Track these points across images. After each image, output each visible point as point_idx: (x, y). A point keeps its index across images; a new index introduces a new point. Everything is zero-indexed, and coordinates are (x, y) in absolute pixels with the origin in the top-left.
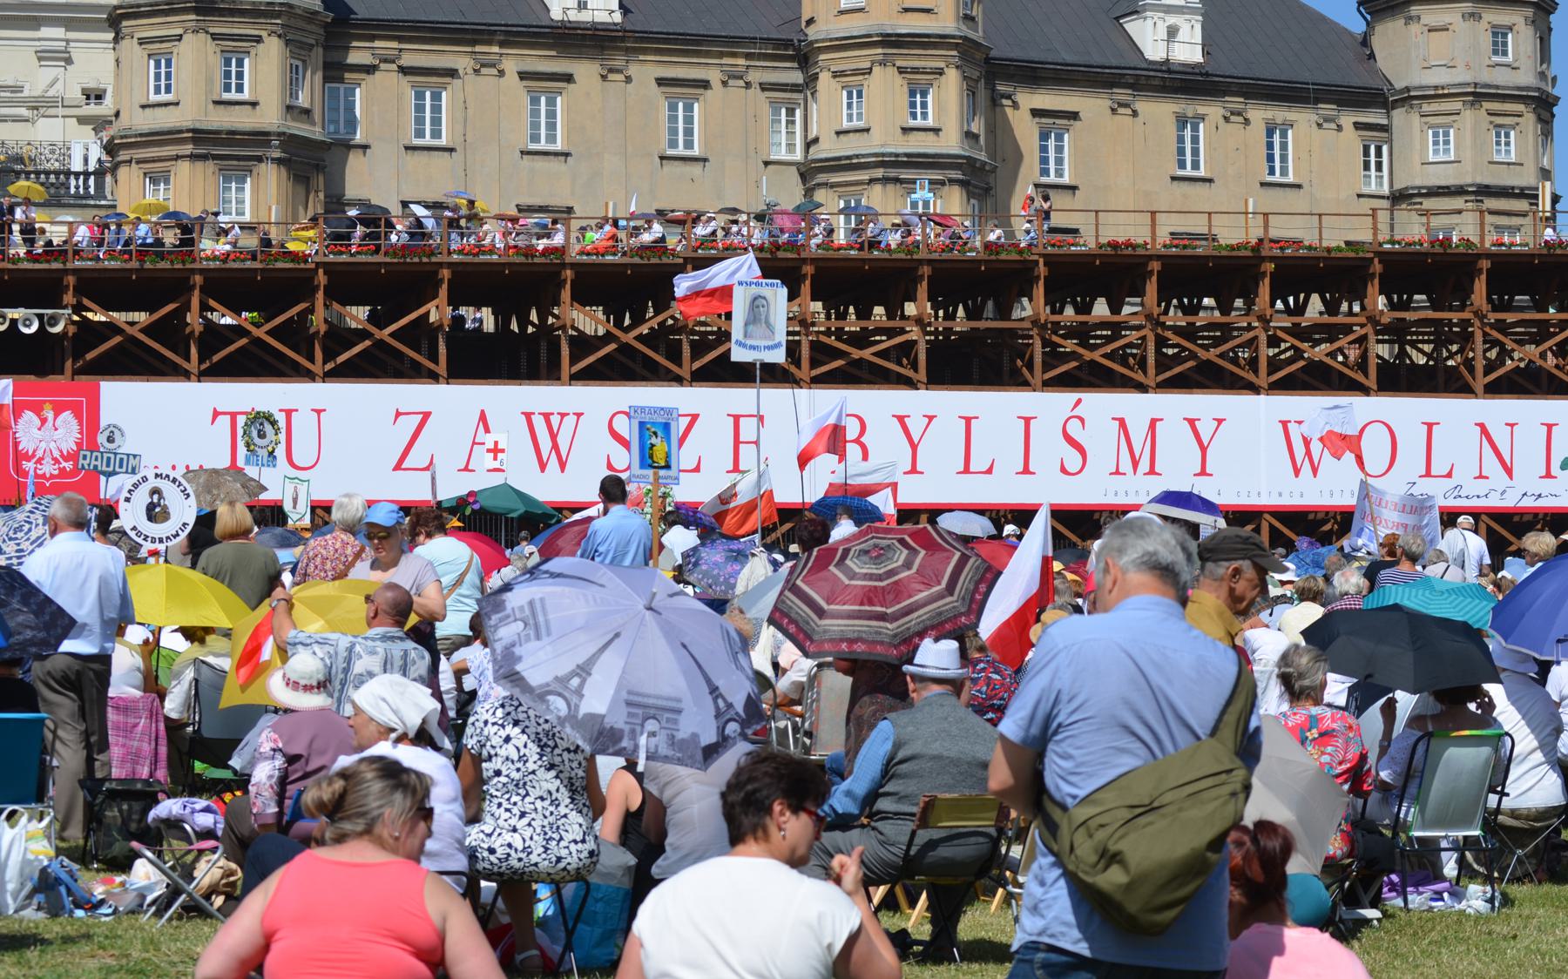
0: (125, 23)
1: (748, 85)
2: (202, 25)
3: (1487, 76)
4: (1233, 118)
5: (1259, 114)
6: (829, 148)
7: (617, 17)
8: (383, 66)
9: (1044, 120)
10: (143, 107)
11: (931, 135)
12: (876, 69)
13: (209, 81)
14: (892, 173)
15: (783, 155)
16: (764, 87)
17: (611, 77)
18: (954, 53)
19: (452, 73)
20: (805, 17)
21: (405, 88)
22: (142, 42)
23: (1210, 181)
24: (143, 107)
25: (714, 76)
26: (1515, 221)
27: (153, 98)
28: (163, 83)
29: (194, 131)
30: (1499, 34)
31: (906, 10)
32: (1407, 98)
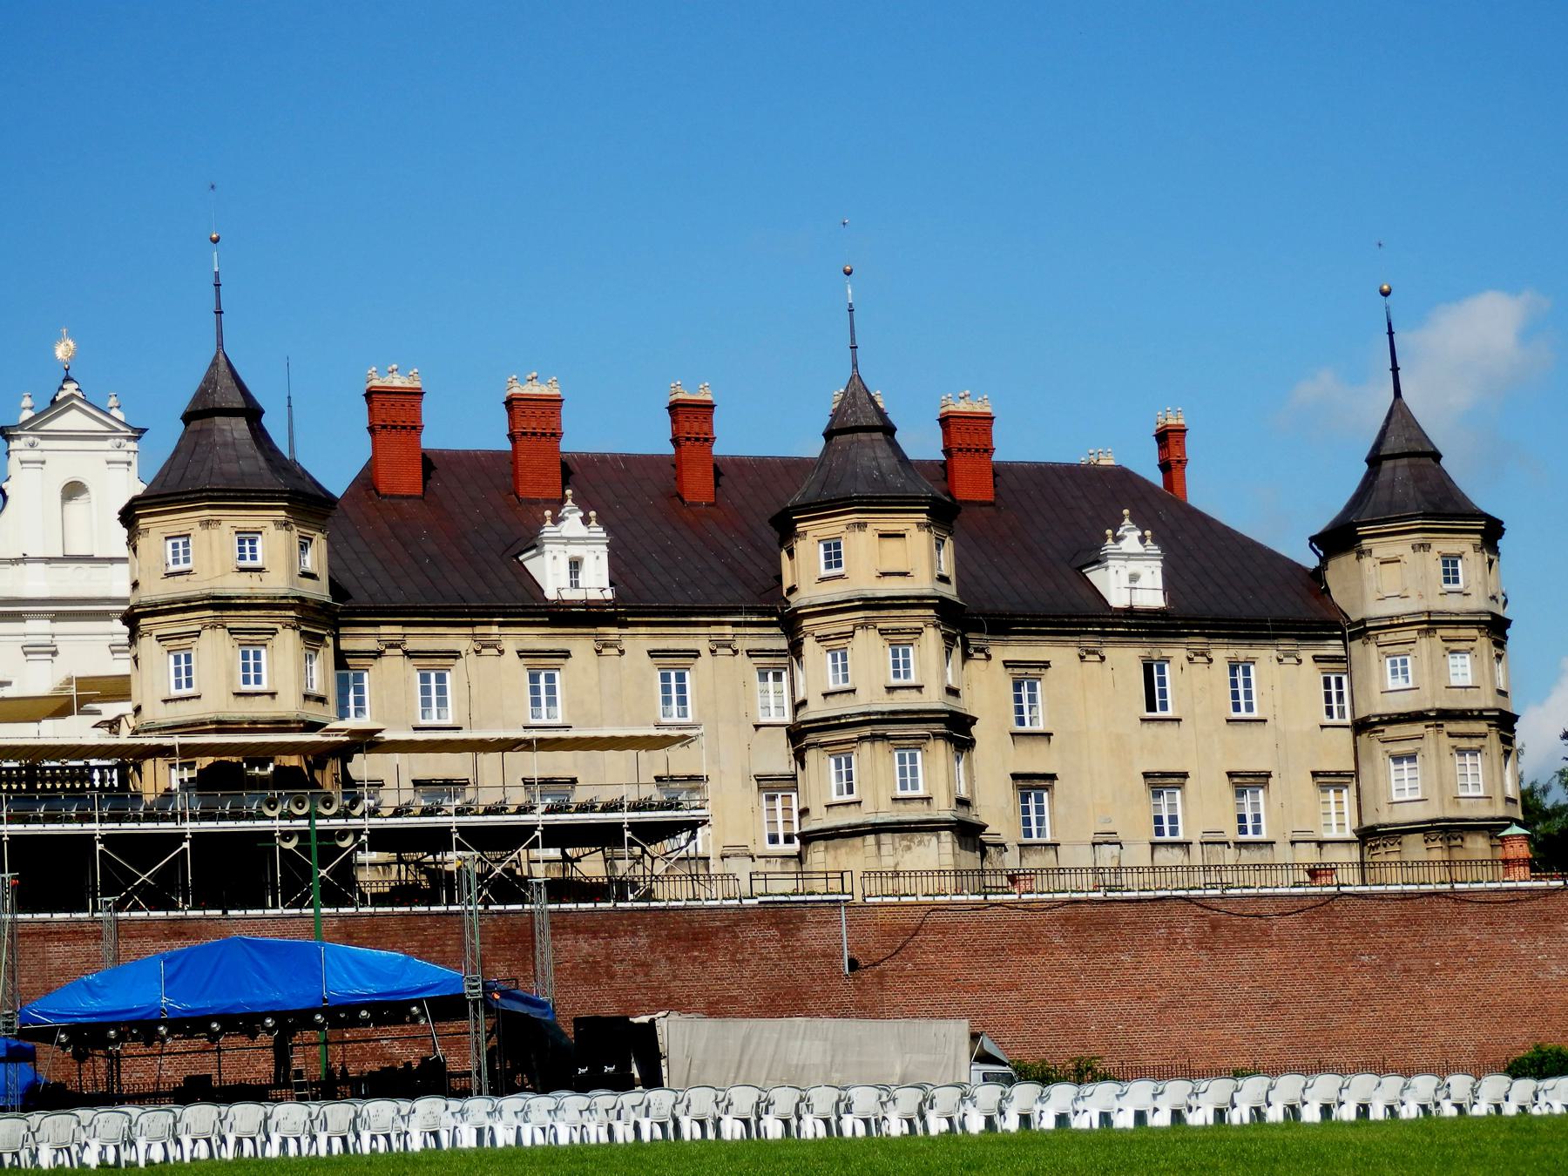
0: (143, 621)
1: (736, 652)
2: (219, 620)
3: (1438, 604)
4: (1197, 659)
5: (1221, 654)
6: (817, 710)
7: (609, 595)
8: (388, 652)
9: (1017, 671)
10: (166, 701)
11: (914, 692)
12: (859, 632)
13: (231, 675)
14: (880, 729)
15: (773, 719)
16: (751, 654)
17: (605, 651)
18: (932, 612)
19: (455, 655)
20: (787, 583)
21: (411, 673)
22: (160, 638)
23: (1179, 720)
24: (166, 701)
25: (703, 645)
26: (1475, 743)
27: (175, 693)
28: (183, 677)
29: (219, 722)
30: (1450, 564)
31: (884, 574)
32: (1361, 631)
